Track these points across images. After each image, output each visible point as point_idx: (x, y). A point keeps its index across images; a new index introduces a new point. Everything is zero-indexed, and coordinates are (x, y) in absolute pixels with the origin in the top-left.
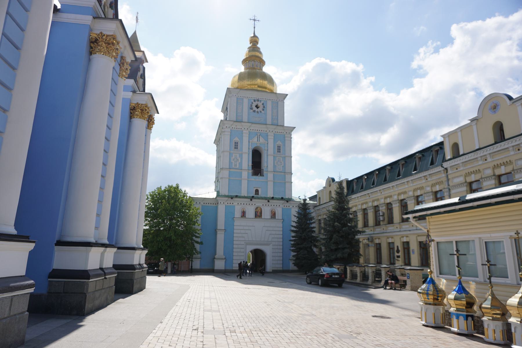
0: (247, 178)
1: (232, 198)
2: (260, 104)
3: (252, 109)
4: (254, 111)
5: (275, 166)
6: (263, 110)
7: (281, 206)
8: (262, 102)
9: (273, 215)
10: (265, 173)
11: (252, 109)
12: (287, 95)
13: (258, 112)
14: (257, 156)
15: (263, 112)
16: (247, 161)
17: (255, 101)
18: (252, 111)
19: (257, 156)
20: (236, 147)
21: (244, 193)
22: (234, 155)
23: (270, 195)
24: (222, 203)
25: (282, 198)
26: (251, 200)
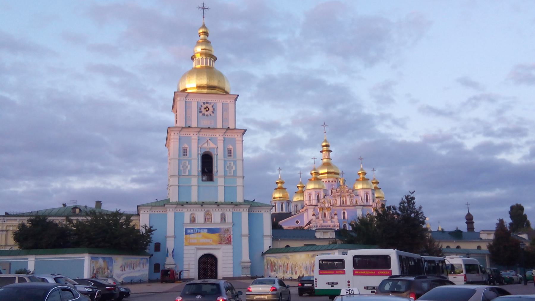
0: (197, 184)
1: (182, 205)
2: (210, 107)
3: (201, 112)
4: (204, 115)
5: (225, 171)
6: (213, 112)
7: (231, 210)
8: (212, 105)
9: (223, 218)
10: (215, 178)
11: (201, 112)
12: (238, 95)
13: (207, 115)
14: (207, 160)
15: (212, 114)
16: (196, 166)
17: (204, 103)
18: (201, 114)
19: (207, 160)
20: (185, 154)
21: (194, 198)
22: (183, 162)
23: (221, 198)
24: (171, 210)
25: (232, 203)
26: (202, 206)
